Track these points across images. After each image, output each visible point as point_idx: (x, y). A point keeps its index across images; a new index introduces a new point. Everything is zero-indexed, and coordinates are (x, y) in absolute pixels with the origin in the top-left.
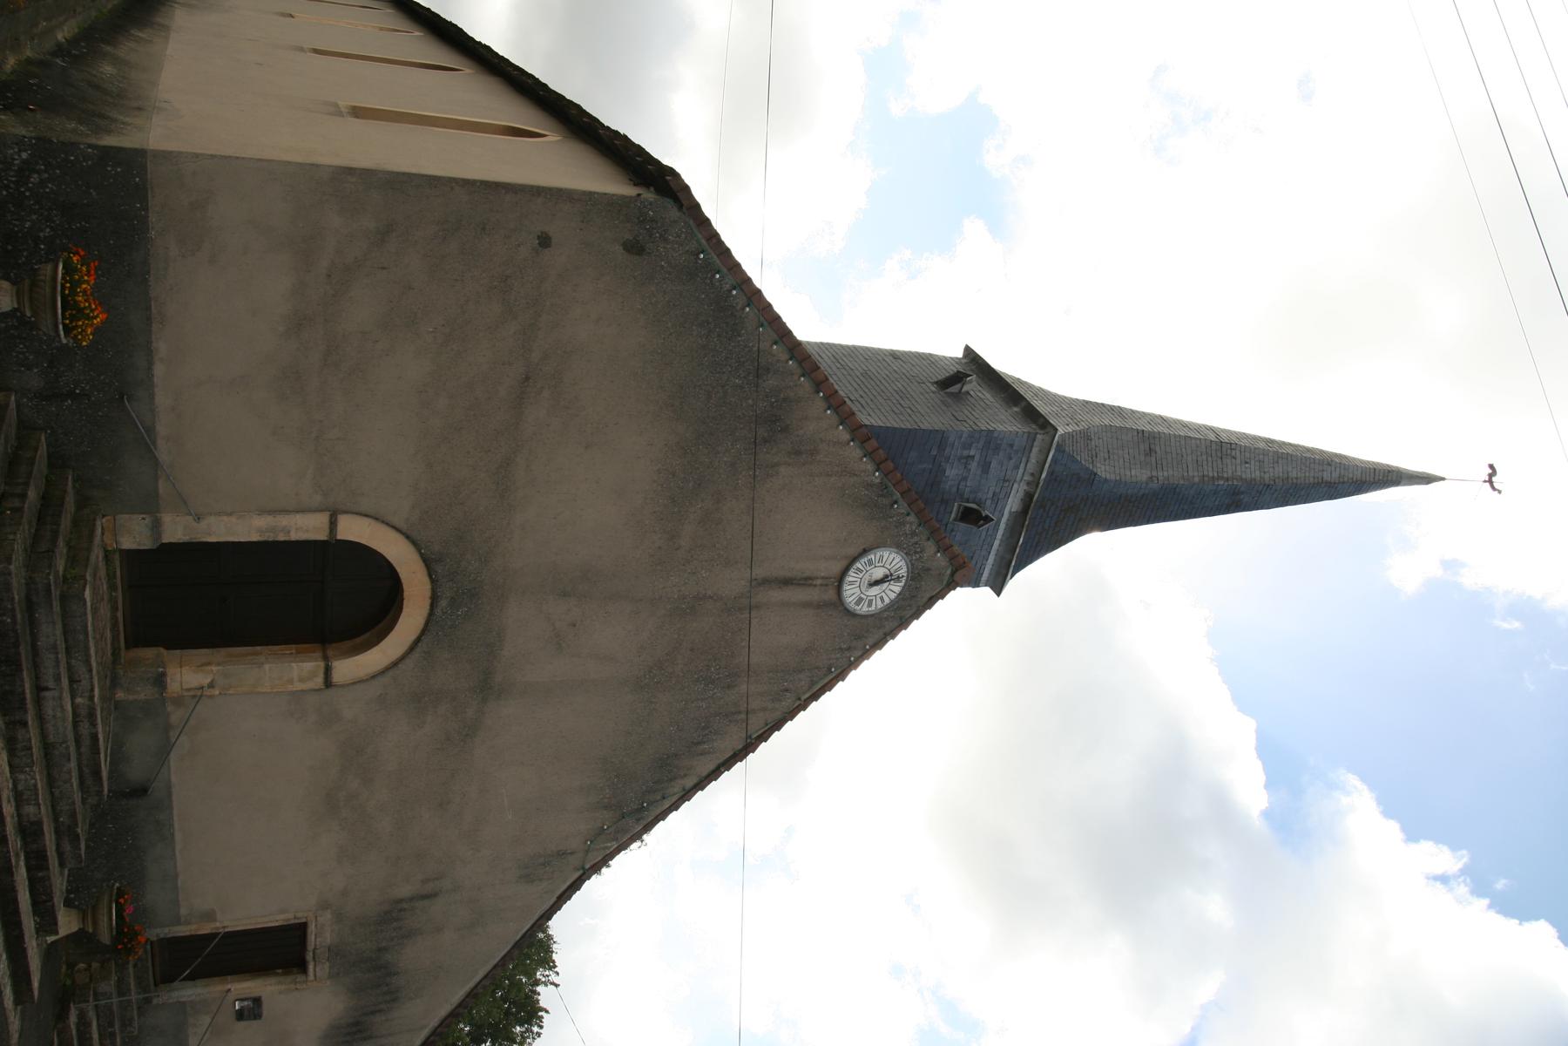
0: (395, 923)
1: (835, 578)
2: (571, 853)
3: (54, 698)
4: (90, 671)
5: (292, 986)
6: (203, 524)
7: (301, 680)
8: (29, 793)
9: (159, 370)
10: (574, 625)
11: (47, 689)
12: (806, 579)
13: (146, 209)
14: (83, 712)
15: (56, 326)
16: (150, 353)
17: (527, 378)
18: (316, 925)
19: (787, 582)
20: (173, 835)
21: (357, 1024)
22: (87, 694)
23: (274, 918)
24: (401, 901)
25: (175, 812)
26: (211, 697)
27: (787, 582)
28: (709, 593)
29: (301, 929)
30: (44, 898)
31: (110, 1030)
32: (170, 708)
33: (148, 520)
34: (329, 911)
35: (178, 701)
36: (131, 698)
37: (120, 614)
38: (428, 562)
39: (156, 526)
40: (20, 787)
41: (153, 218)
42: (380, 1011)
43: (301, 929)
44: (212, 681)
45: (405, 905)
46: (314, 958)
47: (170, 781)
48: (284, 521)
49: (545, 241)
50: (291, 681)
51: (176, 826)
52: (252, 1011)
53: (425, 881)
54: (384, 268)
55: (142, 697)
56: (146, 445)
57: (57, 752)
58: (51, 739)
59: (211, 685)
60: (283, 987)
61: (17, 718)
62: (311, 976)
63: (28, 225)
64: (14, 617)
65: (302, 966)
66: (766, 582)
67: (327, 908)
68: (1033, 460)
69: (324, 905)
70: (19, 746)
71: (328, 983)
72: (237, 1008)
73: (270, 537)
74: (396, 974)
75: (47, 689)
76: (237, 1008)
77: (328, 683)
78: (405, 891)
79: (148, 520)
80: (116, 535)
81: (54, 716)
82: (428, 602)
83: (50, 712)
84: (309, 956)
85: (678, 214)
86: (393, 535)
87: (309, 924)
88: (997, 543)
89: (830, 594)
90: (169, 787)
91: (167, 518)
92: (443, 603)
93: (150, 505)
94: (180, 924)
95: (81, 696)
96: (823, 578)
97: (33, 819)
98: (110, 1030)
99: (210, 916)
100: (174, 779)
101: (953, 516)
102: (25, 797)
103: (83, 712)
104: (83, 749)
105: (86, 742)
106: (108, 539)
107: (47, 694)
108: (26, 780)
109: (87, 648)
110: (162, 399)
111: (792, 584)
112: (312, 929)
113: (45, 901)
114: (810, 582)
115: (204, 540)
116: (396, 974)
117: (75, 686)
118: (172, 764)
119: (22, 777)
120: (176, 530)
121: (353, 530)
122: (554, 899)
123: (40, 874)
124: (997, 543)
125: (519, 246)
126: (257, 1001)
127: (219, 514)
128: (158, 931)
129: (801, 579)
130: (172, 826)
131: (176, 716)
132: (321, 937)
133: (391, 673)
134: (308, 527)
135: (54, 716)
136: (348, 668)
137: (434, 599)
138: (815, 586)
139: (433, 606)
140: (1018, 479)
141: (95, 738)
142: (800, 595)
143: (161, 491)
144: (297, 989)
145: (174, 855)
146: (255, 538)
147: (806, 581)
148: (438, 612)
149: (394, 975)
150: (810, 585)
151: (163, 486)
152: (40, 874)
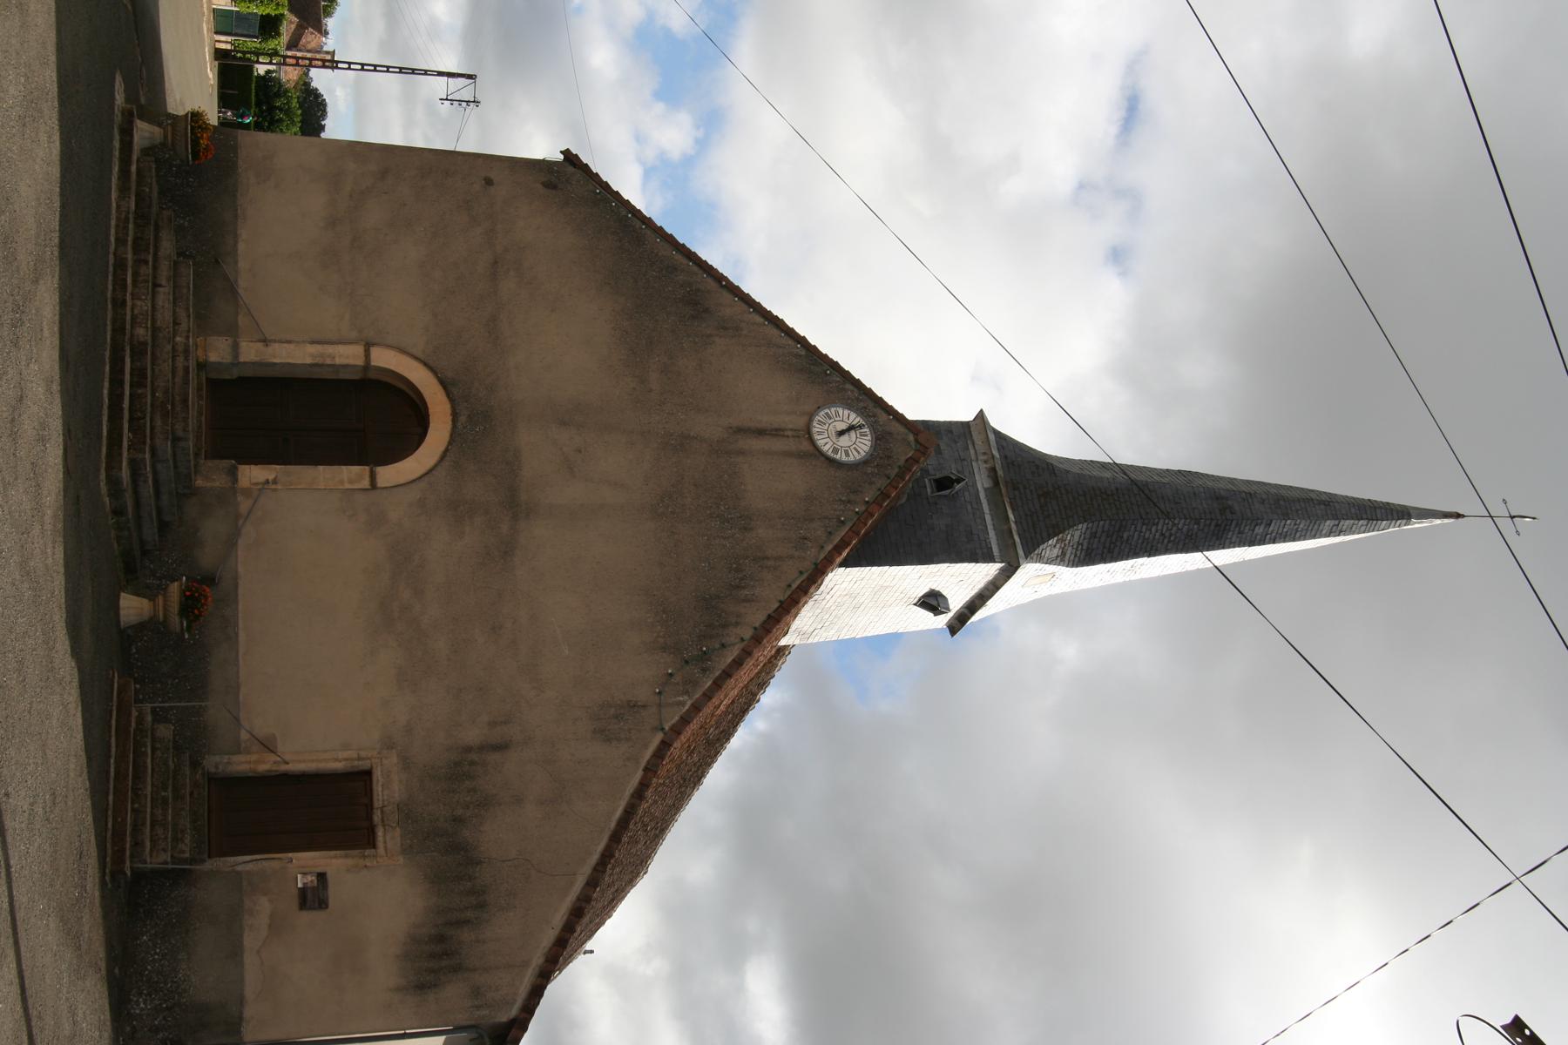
0: (467, 782)
1: (803, 431)
2: (644, 706)
3: (164, 293)
4: (189, 316)
5: (361, 862)
6: (270, 350)
7: (351, 482)
8: (141, 317)
9: (241, 247)
10: (580, 451)
11: (160, 286)
12: (776, 430)
13: (237, 158)
14: (180, 348)
15: (187, 126)
16: (236, 237)
17: (496, 262)
18: (382, 771)
19: (761, 432)
20: (237, 634)
21: (441, 939)
22: (184, 334)
23: (335, 763)
24: (469, 749)
25: (240, 607)
26: (275, 490)
27: (761, 432)
28: (692, 434)
29: (362, 777)
30: (139, 414)
31: (163, 794)
32: (240, 498)
33: (230, 340)
34: (394, 751)
35: (247, 492)
36: (209, 485)
37: (203, 418)
38: (443, 383)
39: (235, 347)
40: (136, 312)
41: (240, 162)
42: (467, 922)
43: (362, 777)
44: (276, 477)
45: (474, 757)
46: (383, 821)
47: (237, 572)
48: (330, 349)
49: (489, 182)
50: (342, 482)
51: (241, 624)
52: (314, 898)
53: (492, 724)
54: (386, 193)
55: (217, 484)
56: (232, 291)
57: (161, 335)
58: (158, 323)
59: (275, 482)
60: (350, 862)
61: (143, 257)
62: (381, 850)
63: (167, 156)
64: (151, 188)
65: (371, 843)
66: (741, 431)
67: (392, 748)
68: (978, 442)
69: (388, 744)
70: (140, 279)
71: (401, 860)
72: (300, 885)
73: (318, 360)
74: (480, 863)
75: (160, 286)
76: (300, 885)
77: (373, 485)
78: (473, 735)
79: (230, 340)
80: (205, 351)
81: (163, 307)
82: (449, 419)
83: (160, 303)
84: (377, 818)
85: (574, 169)
86: (415, 364)
87: (374, 770)
88: (988, 518)
89: (805, 446)
90: (235, 579)
91: (244, 345)
92: (463, 419)
93: (232, 331)
94: (240, 753)
95: (180, 336)
96: (791, 430)
97: (142, 339)
98: (163, 794)
99: (268, 746)
100: (241, 570)
101: (929, 490)
102: (139, 320)
103: (180, 348)
104: (176, 380)
105: (180, 373)
106: (200, 353)
107: (161, 289)
108: (141, 307)
109: (188, 299)
110: (243, 265)
111: (766, 434)
112: (378, 775)
113: (140, 418)
114: (782, 433)
115: (271, 361)
116: (480, 863)
117: (177, 328)
118: (239, 553)
119: (139, 303)
120: (250, 352)
121: (385, 359)
122: (639, 775)
123: (140, 391)
124: (988, 518)
125: (472, 183)
126: (322, 877)
127: (281, 342)
128: (217, 759)
129: (772, 430)
130: (236, 624)
131: (244, 505)
132: (388, 789)
133: (426, 479)
134: (348, 355)
135: (163, 307)
136: (389, 474)
137: (455, 415)
138: (788, 436)
139: (454, 421)
140: (973, 457)
141: (186, 369)
142: (778, 445)
143: (240, 323)
144: (366, 866)
145: (237, 660)
146: (309, 361)
147: (777, 432)
148: (459, 425)
149: (477, 864)
150: (784, 436)
151: (242, 320)
152: (140, 391)
